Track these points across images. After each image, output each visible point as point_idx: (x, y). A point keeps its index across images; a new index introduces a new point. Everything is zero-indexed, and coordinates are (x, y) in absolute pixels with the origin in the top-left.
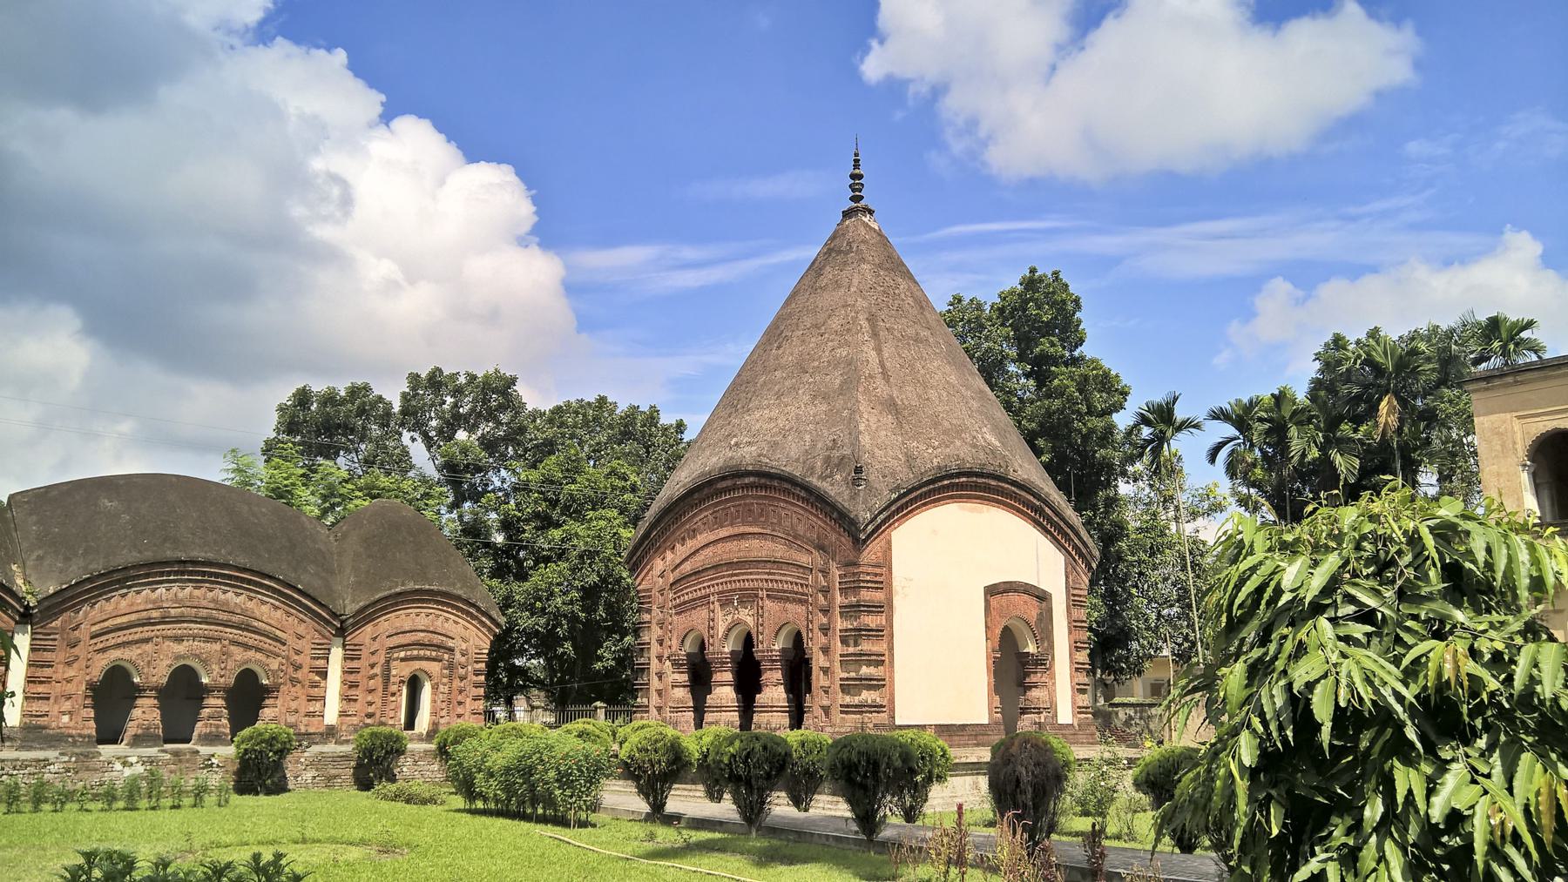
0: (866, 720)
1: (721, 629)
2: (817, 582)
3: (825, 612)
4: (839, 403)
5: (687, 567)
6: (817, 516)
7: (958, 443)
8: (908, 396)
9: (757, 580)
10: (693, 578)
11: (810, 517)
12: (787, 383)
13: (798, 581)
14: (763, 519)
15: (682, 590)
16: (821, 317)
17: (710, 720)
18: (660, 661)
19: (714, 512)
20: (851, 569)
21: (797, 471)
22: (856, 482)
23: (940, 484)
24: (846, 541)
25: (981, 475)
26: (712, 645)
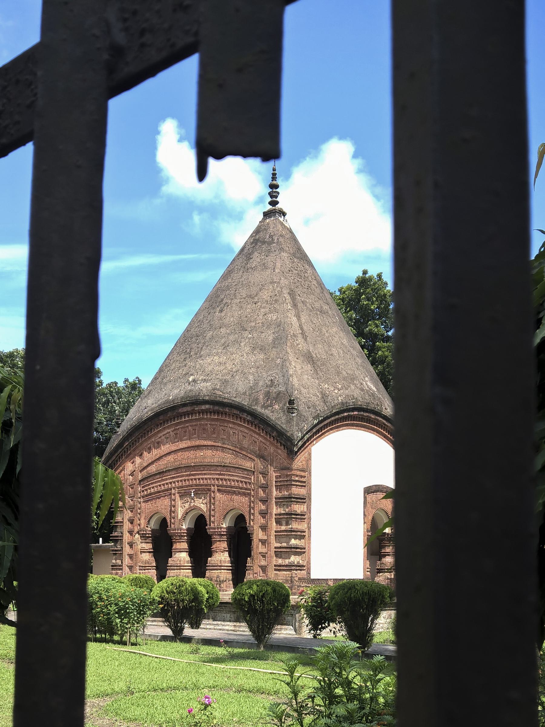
0: (294, 575)
1: (180, 512)
2: (258, 480)
3: (264, 501)
4: (273, 353)
5: (153, 469)
6: (259, 434)
7: (353, 387)
8: (319, 351)
9: (210, 479)
12: (232, 338)
13: (243, 480)
14: (215, 436)
15: (149, 485)
16: (254, 290)
17: (172, 575)
18: (131, 534)
20: (285, 472)
21: (245, 402)
22: (290, 410)
23: (342, 415)
24: (282, 453)
26: (174, 524)
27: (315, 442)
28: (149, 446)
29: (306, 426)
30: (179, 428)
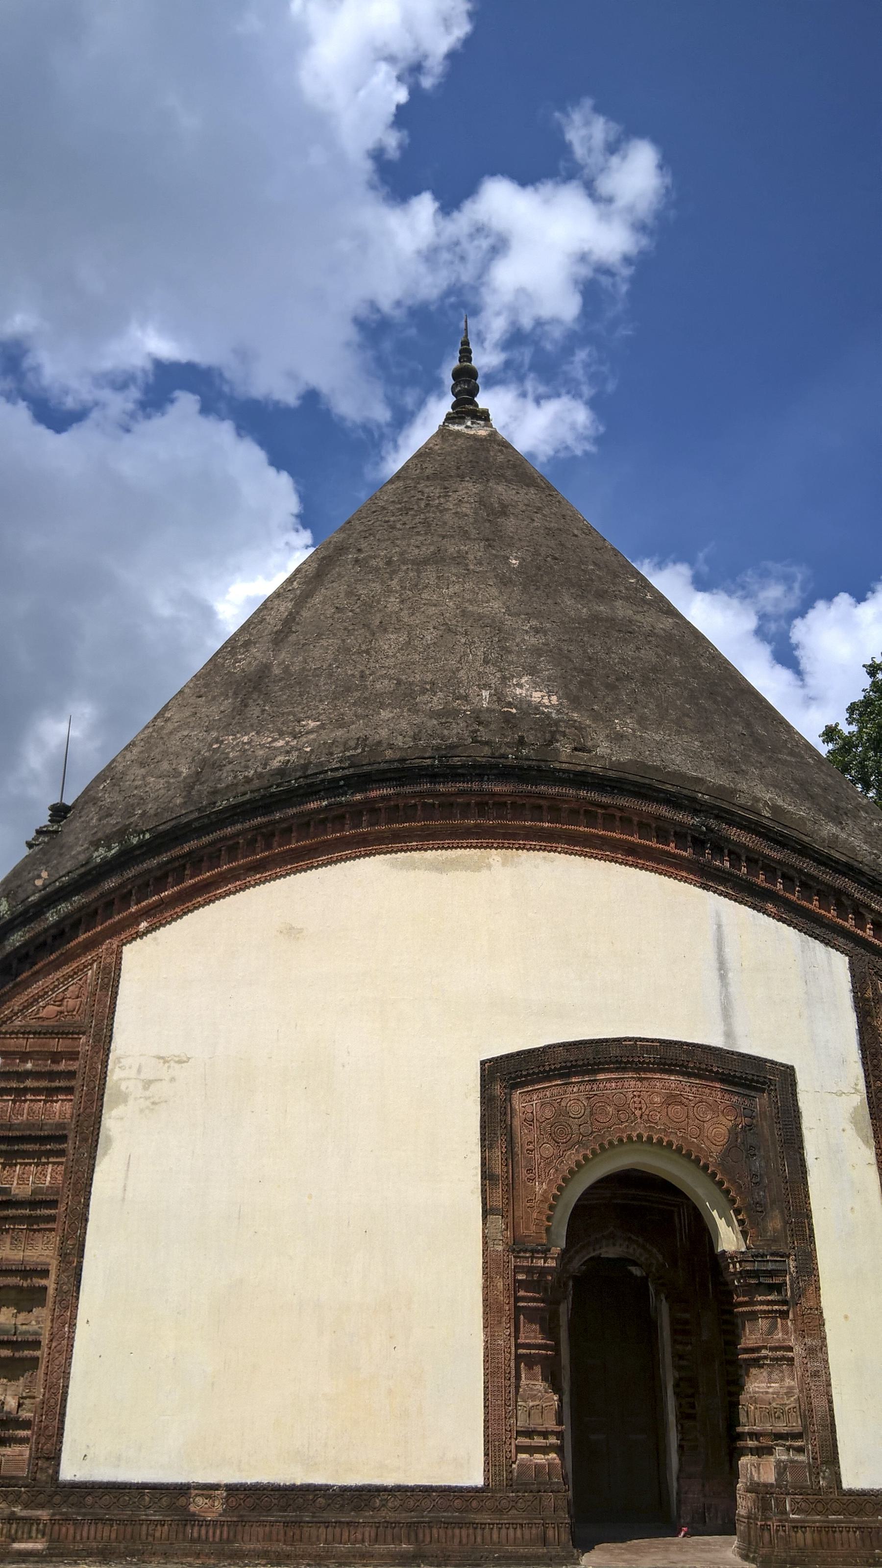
25: (453, 774)
27: (144, 925)
29: (44, 875)
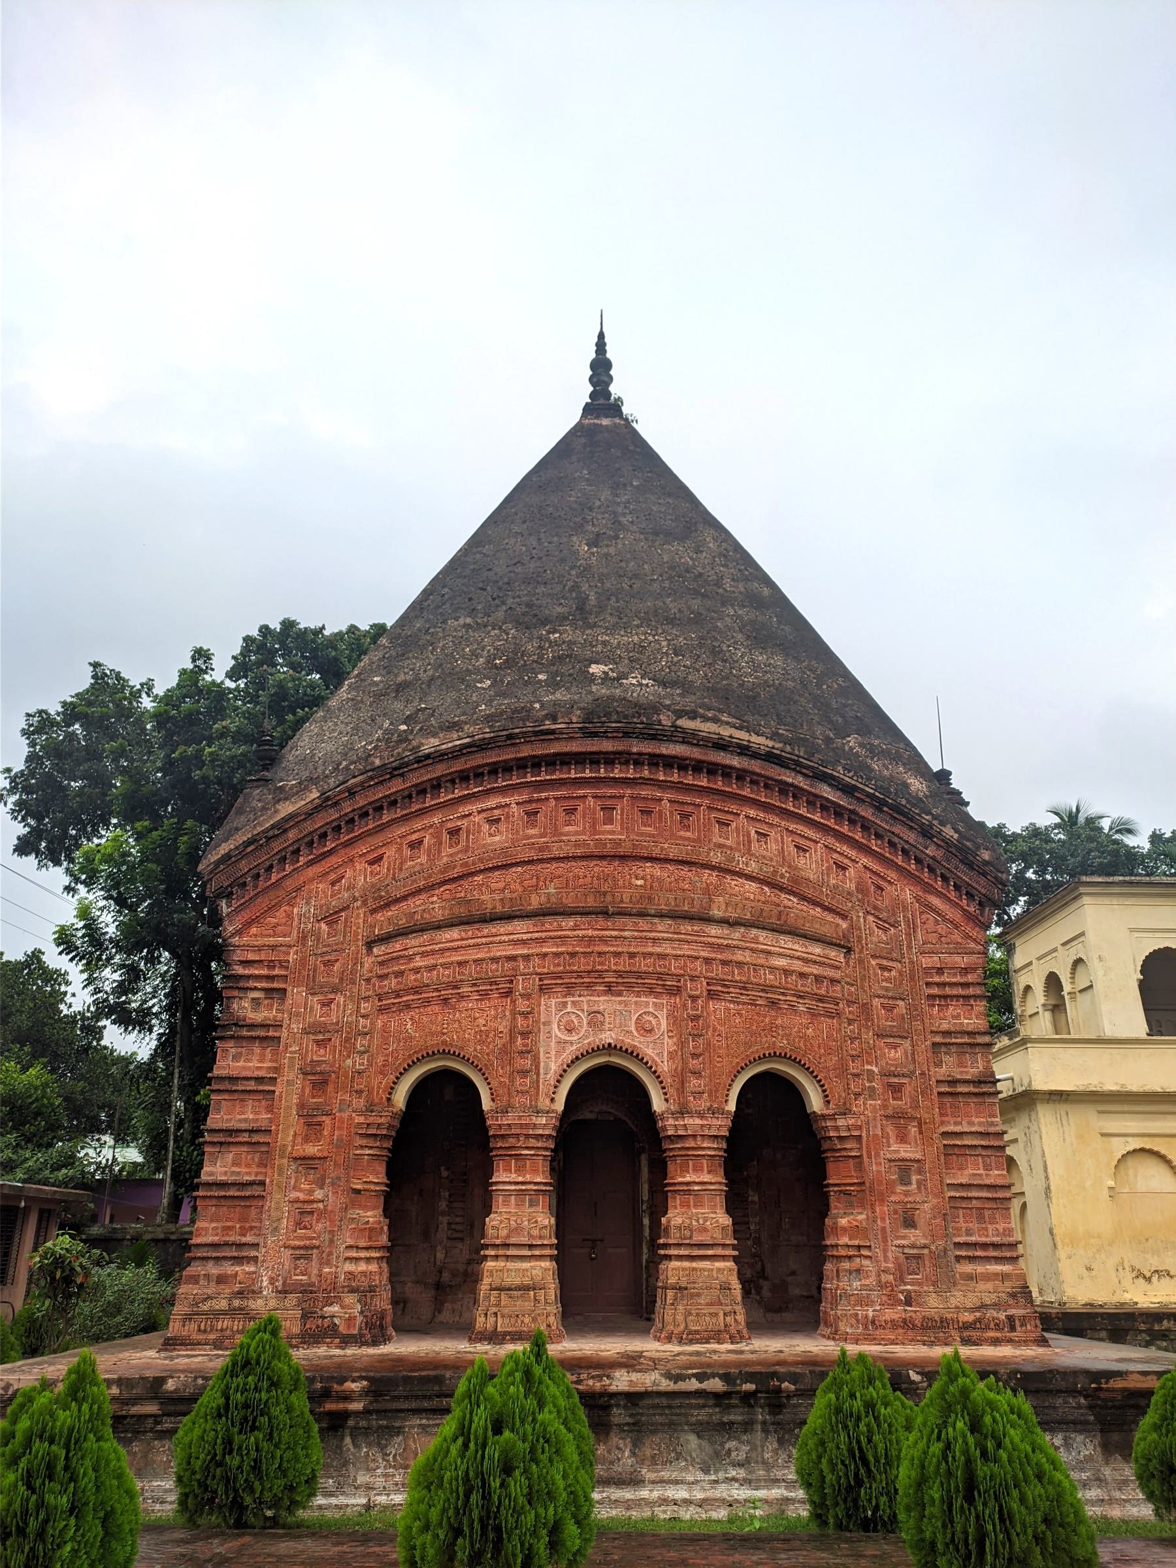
10: (455, 933)
11: (838, 846)
13: (806, 970)
14: (688, 834)
19: (530, 802)
28: (414, 837)
30: (547, 799)
